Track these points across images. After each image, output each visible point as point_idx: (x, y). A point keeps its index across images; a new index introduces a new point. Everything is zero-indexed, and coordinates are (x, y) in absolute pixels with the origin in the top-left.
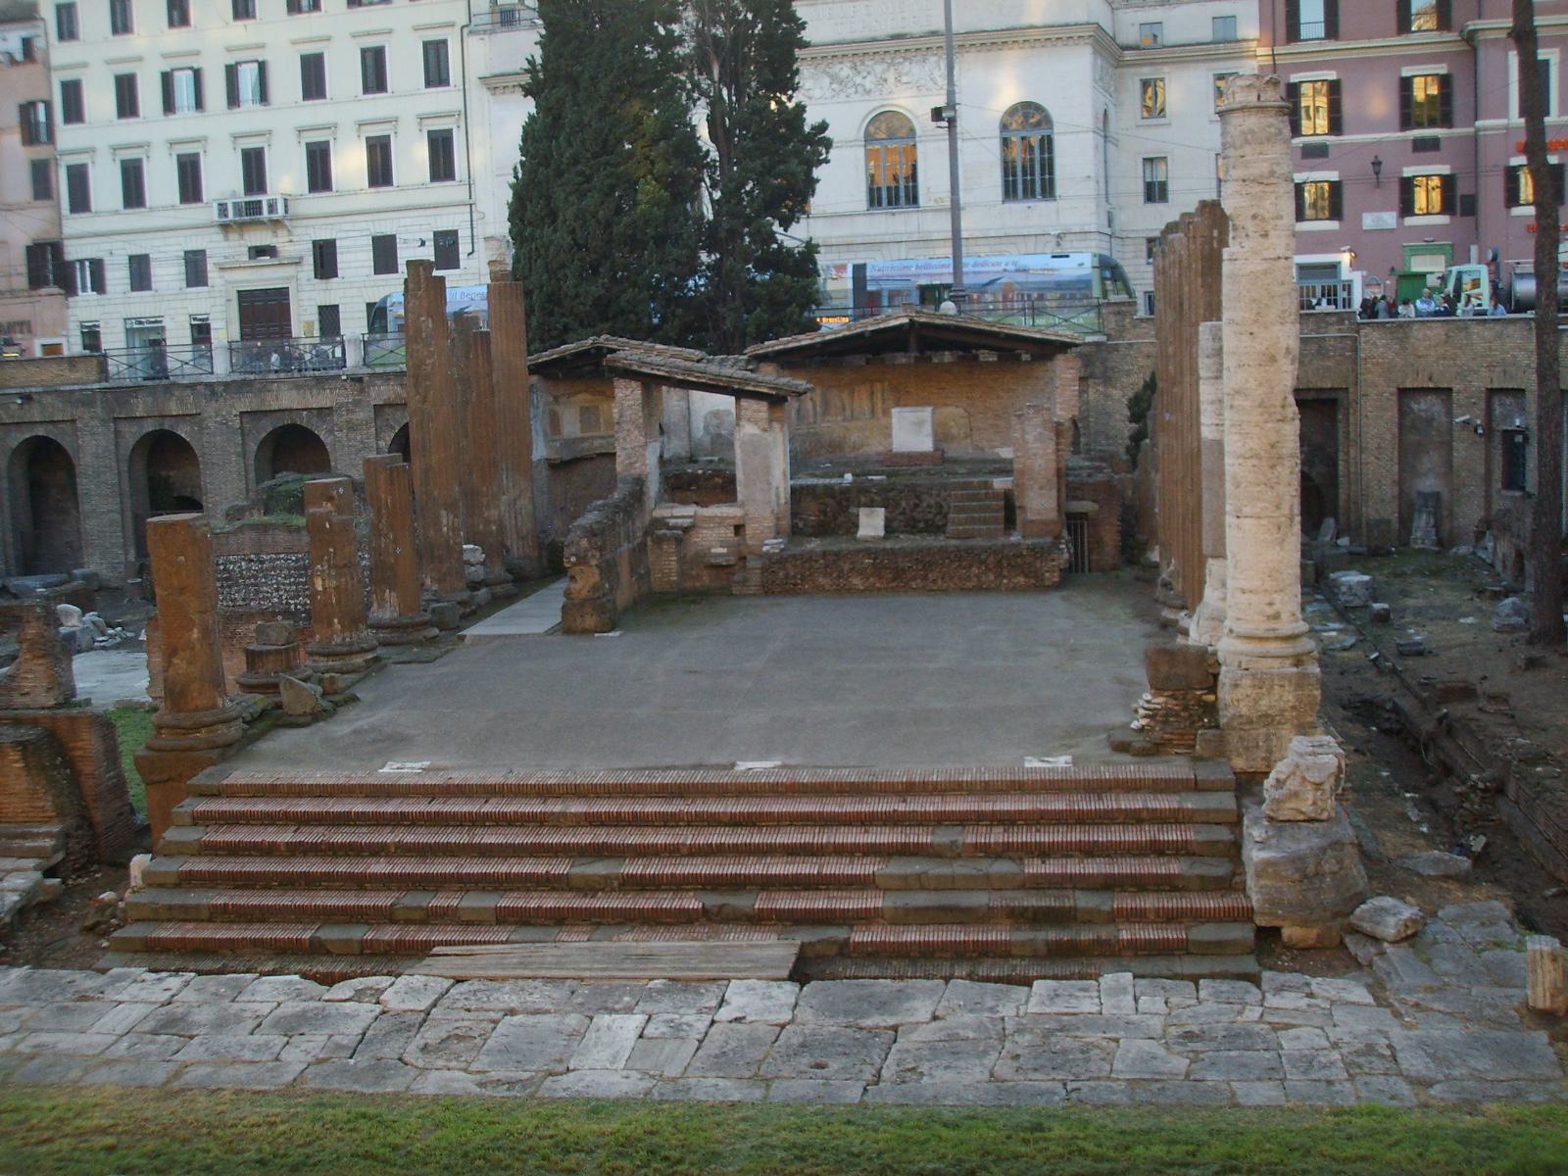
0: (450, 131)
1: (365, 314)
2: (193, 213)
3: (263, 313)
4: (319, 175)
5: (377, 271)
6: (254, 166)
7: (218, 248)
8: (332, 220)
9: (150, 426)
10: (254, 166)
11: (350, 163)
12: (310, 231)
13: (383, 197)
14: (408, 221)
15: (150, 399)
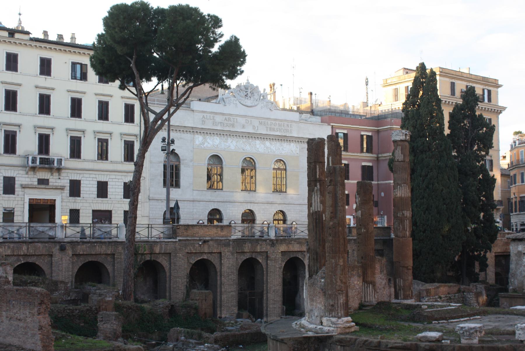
0: (133, 142)
1: (91, 215)
2: (9, 159)
3: (42, 211)
4: (76, 150)
5: (98, 197)
6: (44, 142)
7: (22, 178)
8: (103, 173)
9: (248, 256)
10: (44, 142)
11: (89, 148)
12: (69, 175)
13: (103, 165)
14: (114, 177)
15: (250, 245)
